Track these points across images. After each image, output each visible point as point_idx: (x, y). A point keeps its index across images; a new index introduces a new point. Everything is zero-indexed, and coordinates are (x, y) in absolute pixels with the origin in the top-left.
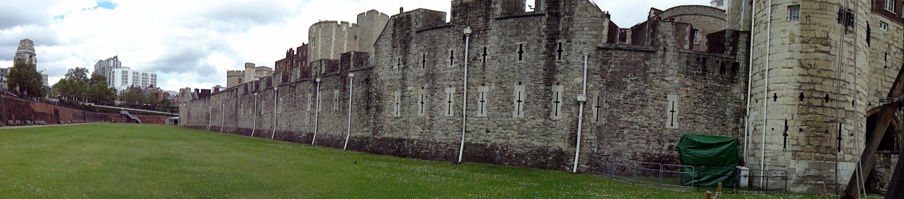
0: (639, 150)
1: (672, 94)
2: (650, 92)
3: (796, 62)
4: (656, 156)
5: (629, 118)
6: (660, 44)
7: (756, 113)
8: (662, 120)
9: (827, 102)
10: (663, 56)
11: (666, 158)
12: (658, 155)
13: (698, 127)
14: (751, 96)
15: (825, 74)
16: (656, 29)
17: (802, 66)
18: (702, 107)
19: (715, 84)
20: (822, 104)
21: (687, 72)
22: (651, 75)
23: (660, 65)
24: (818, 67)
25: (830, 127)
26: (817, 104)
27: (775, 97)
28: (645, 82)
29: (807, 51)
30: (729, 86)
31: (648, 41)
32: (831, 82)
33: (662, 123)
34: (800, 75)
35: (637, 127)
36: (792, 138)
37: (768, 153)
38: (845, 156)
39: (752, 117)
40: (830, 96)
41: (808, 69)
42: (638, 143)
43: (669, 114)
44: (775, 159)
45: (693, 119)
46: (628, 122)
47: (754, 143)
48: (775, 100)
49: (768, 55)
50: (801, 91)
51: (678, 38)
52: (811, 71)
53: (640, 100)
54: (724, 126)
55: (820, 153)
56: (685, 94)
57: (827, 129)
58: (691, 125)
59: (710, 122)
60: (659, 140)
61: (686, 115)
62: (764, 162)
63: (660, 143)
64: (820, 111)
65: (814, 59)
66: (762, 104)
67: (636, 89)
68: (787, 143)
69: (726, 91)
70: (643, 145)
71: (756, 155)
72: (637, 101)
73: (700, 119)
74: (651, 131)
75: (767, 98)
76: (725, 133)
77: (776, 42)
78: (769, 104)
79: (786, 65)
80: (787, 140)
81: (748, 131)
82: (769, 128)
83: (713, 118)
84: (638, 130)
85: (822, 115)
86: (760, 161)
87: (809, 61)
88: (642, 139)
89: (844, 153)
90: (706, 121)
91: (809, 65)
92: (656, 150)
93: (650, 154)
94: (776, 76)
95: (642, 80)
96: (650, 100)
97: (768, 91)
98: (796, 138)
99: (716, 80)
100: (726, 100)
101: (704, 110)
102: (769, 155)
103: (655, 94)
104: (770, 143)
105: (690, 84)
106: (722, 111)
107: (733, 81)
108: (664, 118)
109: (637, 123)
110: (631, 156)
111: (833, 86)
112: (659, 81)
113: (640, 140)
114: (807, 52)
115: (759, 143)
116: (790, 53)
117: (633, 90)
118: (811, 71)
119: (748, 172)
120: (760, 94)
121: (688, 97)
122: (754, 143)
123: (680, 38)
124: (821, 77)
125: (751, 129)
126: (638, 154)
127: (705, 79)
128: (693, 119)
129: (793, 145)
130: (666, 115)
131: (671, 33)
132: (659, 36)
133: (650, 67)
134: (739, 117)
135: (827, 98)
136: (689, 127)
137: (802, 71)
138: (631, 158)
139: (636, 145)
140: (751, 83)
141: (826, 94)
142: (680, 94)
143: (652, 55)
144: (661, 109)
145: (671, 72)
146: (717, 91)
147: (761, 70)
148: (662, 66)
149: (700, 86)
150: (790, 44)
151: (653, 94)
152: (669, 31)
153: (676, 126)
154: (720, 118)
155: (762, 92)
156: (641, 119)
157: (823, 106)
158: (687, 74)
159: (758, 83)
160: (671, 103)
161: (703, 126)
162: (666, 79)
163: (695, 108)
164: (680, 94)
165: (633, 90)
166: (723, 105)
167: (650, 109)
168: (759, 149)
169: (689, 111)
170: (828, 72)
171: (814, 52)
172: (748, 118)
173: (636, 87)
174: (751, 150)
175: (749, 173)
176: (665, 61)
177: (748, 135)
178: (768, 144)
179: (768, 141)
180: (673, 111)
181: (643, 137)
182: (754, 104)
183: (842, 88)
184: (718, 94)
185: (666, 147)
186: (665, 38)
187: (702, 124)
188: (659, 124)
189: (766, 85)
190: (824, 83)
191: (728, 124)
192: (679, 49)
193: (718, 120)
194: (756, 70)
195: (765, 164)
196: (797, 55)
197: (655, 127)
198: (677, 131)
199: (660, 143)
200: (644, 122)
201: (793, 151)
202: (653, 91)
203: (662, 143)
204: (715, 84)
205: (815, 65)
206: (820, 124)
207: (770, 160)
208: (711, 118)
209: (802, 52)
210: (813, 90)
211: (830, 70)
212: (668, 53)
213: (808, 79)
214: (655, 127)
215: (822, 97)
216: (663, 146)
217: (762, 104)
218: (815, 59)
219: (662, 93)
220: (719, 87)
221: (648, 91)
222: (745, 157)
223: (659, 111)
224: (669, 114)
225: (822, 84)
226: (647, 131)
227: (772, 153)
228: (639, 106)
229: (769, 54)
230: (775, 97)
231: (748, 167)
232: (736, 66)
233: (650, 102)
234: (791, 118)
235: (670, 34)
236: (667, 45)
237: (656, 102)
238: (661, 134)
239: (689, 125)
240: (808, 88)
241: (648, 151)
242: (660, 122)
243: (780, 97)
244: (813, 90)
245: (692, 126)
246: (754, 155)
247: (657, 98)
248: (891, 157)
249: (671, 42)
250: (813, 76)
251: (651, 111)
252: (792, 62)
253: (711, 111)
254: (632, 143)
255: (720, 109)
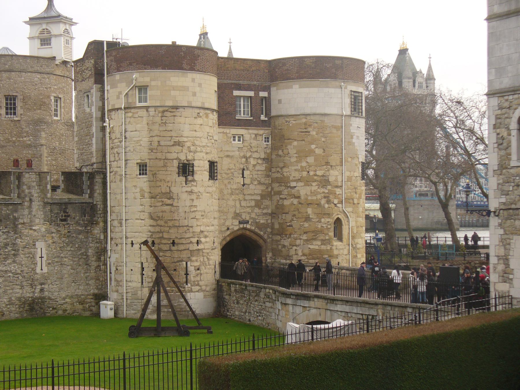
0: (14, 295)
1: (40, 241)
2: (21, 242)
3: (146, 215)
4: (30, 299)
5: (3, 267)
6: (26, 196)
7: (117, 256)
8: (33, 266)
9: (174, 246)
10: (30, 207)
11: (39, 299)
12: (32, 297)
13: (65, 268)
14: (111, 239)
15: (170, 224)
16: (21, 181)
17: (152, 218)
18: (67, 250)
19: (77, 228)
20: (170, 249)
21: (51, 220)
22: (20, 226)
23: (28, 216)
24: (165, 218)
25: (178, 266)
26: (166, 249)
27: (132, 244)
28: (15, 233)
29: (155, 205)
30: (89, 228)
31: (14, 193)
32: (176, 230)
33: (33, 268)
34: (150, 226)
35: (11, 274)
36: (148, 277)
37: (129, 289)
38: (193, 287)
39: (112, 258)
40: (175, 241)
41: (156, 220)
42: (12, 289)
43: (39, 260)
44: (135, 294)
45: (60, 262)
46: (3, 271)
47: (116, 280)
48: (132, 246)
49: (124, 207)
50: (152, 239)
51: (41, 187)
52: (159, 222)
53: (12, 250)
54: (87, 266)
55: (170, 287)
56: (51, 240)
57: (175, 268)
58: (58, 268)
59: (75, 263)
60: (31, 284)
61: (54, 259)
62: (126, 296)
63: (32, 287)
64: (168, 254)
65: (161, 212)
66: (122, 248)
67: (8, 240)
68: (144, 281)
69: (87, 232)
70: (18, 291)
71: (119, 291)
72: (9, 251)
73: (65, 261)
74: (24, 277)
75: (126, 244)
76: (89, 271)
77: (130, 196)
78: (127, 249)
79: (138, 218)
80: (144, 279)
81: (110, 270)
82: (129, 269)
83: (77, 259)
84: (12, 278)
85: (170, 257)
86: (122, 296)
87: (157, 213)
88: (16, 285)
89: (191, 286)
90: (72, 263)
91: (157, 217)
92: (29, 293)
93: (24, 298)
94: (132, 226)
95: (13, 231)
96: (21, 249)
97: (126, 238)
98: (150, 276)
99: (78, 223)
100: (88, 242)
101: (69, 253)
102: (129, 290)
103: (25, 243)
104: (130, 281)
105: (54, 231)
106: (85, 252)
107: (92, 223)
108: (34, 264)
109: (11, 271)
110: (7, 302)
111: (178, 232)
112: (27, 231)
113: (15, 286)
114: (155, 206)
115: (121, 281)
116: (141, 207)
117: (5, 241)
118: (159, 222)
119: (113, 306)
120: (120, 239)
121: (54, 243)
122: (116, 280)
123: (43, 187)
124: (168, 226)
125: (113, 269)
126: (13, 299)
127: (67, 224)
128: (60, 262)
129: (149, 282)
130: (36, 262)
131: (35, 183)
132: (25, 187)
133: (19, 218)
134: (100, 255)
135: (173, 243)
136: (57, 270)
137: (152, 222)
138: (8, 303)
139: (11, 291)
140: (111, 227)
141: (172, 240)
142: (47, 241)
143: (20, 207)
144: (31, 256)
145: (37, 221)
146: (79, 234)
147: (119, 218)
148: (29, 216)
149: (64, 231)
150: (141, 199)
151: (23, 243)
152: (34, 182)
153: (45, 270)
154: (84, 258)
155: (121, 238)
156: (13, 268)
157: (170, 250)
158: (51, 222)
159: (117, 230)
160: (39, 250)
161: (69, 267)
162: (34, 228)
163: (61, 252)
164: (47, 241)
165: (5, 241)
166: (85, 246)
167: (22, 258)
168: (121, 286)
169: (55, 255)
170: (173, 222)
171: (161, 206)
172: (110, 258)
173: (7, 239)
174: (114, 287)
175: (114, 306)
176: (32, 211)
177: (111, 273)
178: (129, 282)
179: (128, 280)
180: (42, 257)
181: (17, 283)
182: (114, 248)
183: (186, 232)
184: (80, 236)
185: (38, 290)
186: (30, 189)
187: (68, 266)
188: (30, 270)
189: (124, 233)
190: (171, 231)
191: (91, 263)
192: (43, 198)
193: (82, 260)
194: (114, 216)
195: (127, 298)
196: (148, 209)
197: (27, 273)
198: (46, 275)
199: (32, 287)
200: (17, 270)
201: (149, 287)
202: (23, 241)
203: (34, 287)
204: (77, 228)
205: (162, 217)
206: (169, 264)
207: (130, 295)
208: (75, 259)
209: (151, 206)
210: (162, 238)
211: (175, 220)
212: (33, 203)
213: (157, 229)
214: (27, 273)
215: (169, 242)
216: (35, 289)
217: (122, 248)
218: (162, 212)
219: (31, 242)
220: (81, 230)
221: (19, 241)
222: (108, 293)
223: (29, 258)
224: (39, 260)
225: (169, 232)
226: (20, 278)
227: (132, 289)
228: (12, 256)
229: (125, 206)
230: (132, 244)
231: (113, 301)
232: (93, 207)
233: (21, 251)
234: (146, 261)
235: (34, 184)
236: (33, 196)
237: (27, 251)
238: (33, 279)
239: (56, 268)
240: (157, 236)
241: (23, 295)
242: (31, 268)
243: (136, 244)
244: (162, 238)
245: (59, 269)
246: (117, 291)
247: (28, 246)
248: (231, 287)
249: (35, 193)
250: (161, 226)
251: (22, 259)
252: (143, 215)
253: (75, 253)
254: (7, 289)
255: (83, 250)
